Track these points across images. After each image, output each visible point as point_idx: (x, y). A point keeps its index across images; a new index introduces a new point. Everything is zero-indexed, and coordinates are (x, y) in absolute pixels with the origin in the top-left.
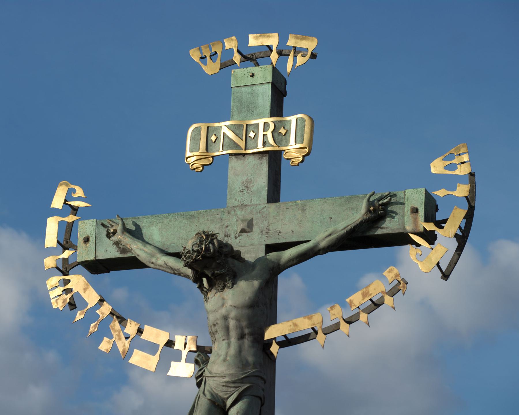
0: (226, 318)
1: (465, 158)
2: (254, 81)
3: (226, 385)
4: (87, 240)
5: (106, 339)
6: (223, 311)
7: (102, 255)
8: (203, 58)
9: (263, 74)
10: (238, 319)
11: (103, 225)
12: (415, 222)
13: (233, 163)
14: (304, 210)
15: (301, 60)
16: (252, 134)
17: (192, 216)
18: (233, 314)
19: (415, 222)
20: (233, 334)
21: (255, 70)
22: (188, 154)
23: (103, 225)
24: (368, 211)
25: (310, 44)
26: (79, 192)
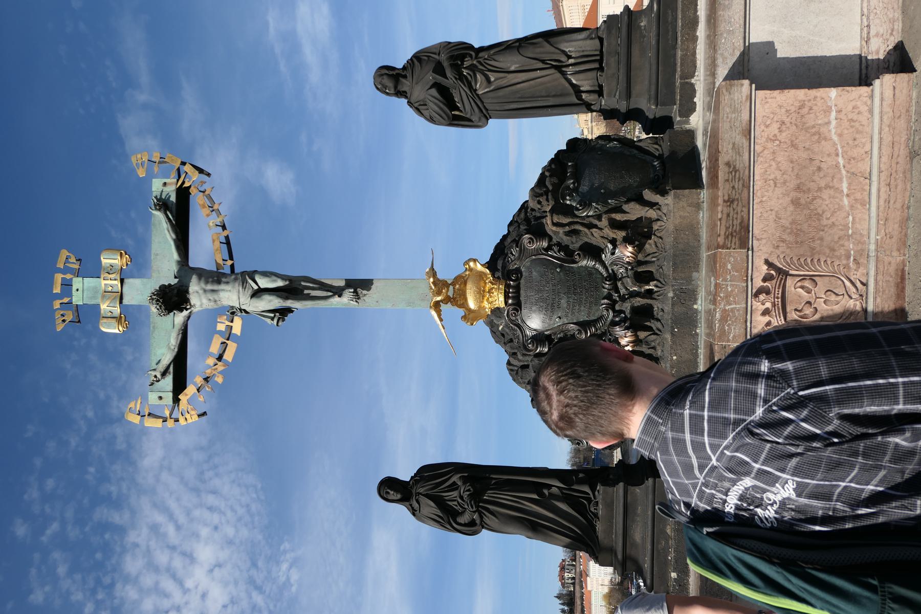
0: (205, 291)
1: (139, 156)
2: (80, 290)
3: (244, 288)
4: (160, 398)
5: (216, 379)
6: (201, 292)
7: (170, 387)
8: (64, 321)
9: (77, 283)
10: (207, 282)
11: (152, 384)
12: (171, 184)
13: (125, 302)
14: (157, 255)
15: (73, 260)
16: (110, 289)
17: (154, 327)
18: (203, 285)
19: (171, 184)
20: (215, 287)
21: (74, 288)
22: (116, 331)
23: (152, 384)
24: (159, 210)
25: (64, 253)
26: (132, 405)
